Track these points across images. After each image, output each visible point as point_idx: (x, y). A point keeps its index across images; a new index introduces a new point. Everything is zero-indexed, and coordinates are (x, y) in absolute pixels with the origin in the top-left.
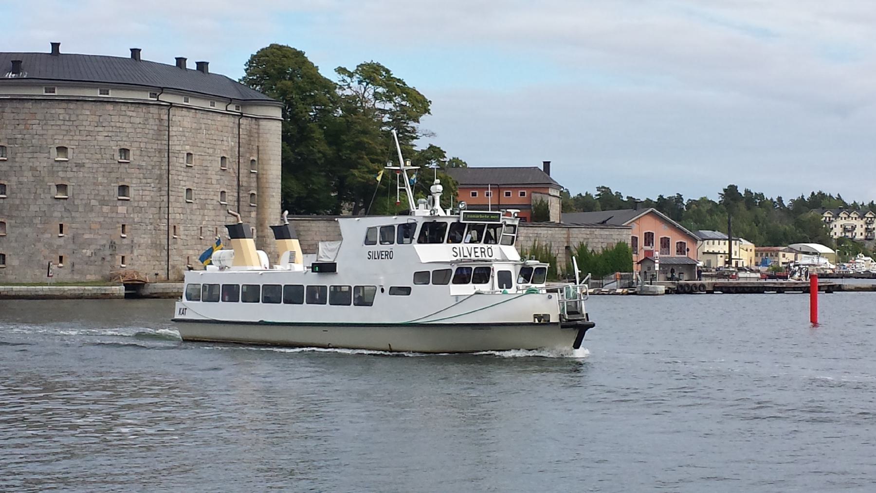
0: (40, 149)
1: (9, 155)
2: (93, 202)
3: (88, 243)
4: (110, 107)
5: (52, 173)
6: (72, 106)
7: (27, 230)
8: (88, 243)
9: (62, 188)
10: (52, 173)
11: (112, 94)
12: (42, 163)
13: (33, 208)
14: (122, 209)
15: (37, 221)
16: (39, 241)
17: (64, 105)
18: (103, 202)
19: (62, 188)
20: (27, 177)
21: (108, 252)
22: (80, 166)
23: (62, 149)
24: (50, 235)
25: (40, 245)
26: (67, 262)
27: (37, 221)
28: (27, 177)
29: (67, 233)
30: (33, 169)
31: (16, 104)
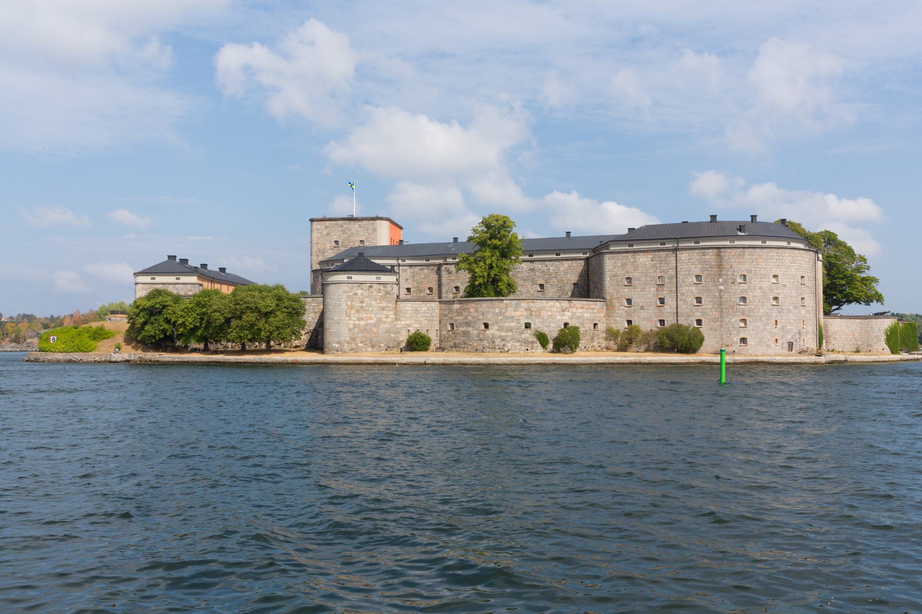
0: (765, 276)
1: (747, 280)
2: (791, 308)
3: (788, 332)
4: (797, 251)
5: (771, 290)
6: (780, 251)
7: (759, 324)
8: (788, 332)
9: (776, 298)
10: (771, 290)
11: (769, 243)
12: (766, 284)
13: (762, 311)
14: (803, 312)
15: (763, 318)
16: (765, 330)
17: (776, 250)
18: (796, 307)
19: (776, 298)
20: (758, 292)
21: (798, 337)
22: (784, 286)
23: (775, 276)
24: (771, 327)
25: (766, 333)
26: (780, 342)
27: (763, 318)
28: (758, 292)
29: (779, 326)
30: (761, 288)
31: (751, 250)
